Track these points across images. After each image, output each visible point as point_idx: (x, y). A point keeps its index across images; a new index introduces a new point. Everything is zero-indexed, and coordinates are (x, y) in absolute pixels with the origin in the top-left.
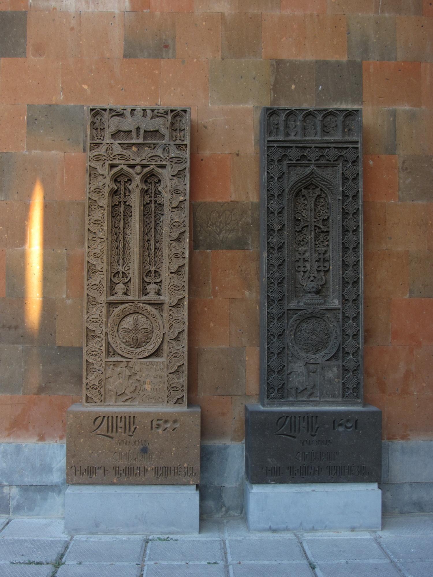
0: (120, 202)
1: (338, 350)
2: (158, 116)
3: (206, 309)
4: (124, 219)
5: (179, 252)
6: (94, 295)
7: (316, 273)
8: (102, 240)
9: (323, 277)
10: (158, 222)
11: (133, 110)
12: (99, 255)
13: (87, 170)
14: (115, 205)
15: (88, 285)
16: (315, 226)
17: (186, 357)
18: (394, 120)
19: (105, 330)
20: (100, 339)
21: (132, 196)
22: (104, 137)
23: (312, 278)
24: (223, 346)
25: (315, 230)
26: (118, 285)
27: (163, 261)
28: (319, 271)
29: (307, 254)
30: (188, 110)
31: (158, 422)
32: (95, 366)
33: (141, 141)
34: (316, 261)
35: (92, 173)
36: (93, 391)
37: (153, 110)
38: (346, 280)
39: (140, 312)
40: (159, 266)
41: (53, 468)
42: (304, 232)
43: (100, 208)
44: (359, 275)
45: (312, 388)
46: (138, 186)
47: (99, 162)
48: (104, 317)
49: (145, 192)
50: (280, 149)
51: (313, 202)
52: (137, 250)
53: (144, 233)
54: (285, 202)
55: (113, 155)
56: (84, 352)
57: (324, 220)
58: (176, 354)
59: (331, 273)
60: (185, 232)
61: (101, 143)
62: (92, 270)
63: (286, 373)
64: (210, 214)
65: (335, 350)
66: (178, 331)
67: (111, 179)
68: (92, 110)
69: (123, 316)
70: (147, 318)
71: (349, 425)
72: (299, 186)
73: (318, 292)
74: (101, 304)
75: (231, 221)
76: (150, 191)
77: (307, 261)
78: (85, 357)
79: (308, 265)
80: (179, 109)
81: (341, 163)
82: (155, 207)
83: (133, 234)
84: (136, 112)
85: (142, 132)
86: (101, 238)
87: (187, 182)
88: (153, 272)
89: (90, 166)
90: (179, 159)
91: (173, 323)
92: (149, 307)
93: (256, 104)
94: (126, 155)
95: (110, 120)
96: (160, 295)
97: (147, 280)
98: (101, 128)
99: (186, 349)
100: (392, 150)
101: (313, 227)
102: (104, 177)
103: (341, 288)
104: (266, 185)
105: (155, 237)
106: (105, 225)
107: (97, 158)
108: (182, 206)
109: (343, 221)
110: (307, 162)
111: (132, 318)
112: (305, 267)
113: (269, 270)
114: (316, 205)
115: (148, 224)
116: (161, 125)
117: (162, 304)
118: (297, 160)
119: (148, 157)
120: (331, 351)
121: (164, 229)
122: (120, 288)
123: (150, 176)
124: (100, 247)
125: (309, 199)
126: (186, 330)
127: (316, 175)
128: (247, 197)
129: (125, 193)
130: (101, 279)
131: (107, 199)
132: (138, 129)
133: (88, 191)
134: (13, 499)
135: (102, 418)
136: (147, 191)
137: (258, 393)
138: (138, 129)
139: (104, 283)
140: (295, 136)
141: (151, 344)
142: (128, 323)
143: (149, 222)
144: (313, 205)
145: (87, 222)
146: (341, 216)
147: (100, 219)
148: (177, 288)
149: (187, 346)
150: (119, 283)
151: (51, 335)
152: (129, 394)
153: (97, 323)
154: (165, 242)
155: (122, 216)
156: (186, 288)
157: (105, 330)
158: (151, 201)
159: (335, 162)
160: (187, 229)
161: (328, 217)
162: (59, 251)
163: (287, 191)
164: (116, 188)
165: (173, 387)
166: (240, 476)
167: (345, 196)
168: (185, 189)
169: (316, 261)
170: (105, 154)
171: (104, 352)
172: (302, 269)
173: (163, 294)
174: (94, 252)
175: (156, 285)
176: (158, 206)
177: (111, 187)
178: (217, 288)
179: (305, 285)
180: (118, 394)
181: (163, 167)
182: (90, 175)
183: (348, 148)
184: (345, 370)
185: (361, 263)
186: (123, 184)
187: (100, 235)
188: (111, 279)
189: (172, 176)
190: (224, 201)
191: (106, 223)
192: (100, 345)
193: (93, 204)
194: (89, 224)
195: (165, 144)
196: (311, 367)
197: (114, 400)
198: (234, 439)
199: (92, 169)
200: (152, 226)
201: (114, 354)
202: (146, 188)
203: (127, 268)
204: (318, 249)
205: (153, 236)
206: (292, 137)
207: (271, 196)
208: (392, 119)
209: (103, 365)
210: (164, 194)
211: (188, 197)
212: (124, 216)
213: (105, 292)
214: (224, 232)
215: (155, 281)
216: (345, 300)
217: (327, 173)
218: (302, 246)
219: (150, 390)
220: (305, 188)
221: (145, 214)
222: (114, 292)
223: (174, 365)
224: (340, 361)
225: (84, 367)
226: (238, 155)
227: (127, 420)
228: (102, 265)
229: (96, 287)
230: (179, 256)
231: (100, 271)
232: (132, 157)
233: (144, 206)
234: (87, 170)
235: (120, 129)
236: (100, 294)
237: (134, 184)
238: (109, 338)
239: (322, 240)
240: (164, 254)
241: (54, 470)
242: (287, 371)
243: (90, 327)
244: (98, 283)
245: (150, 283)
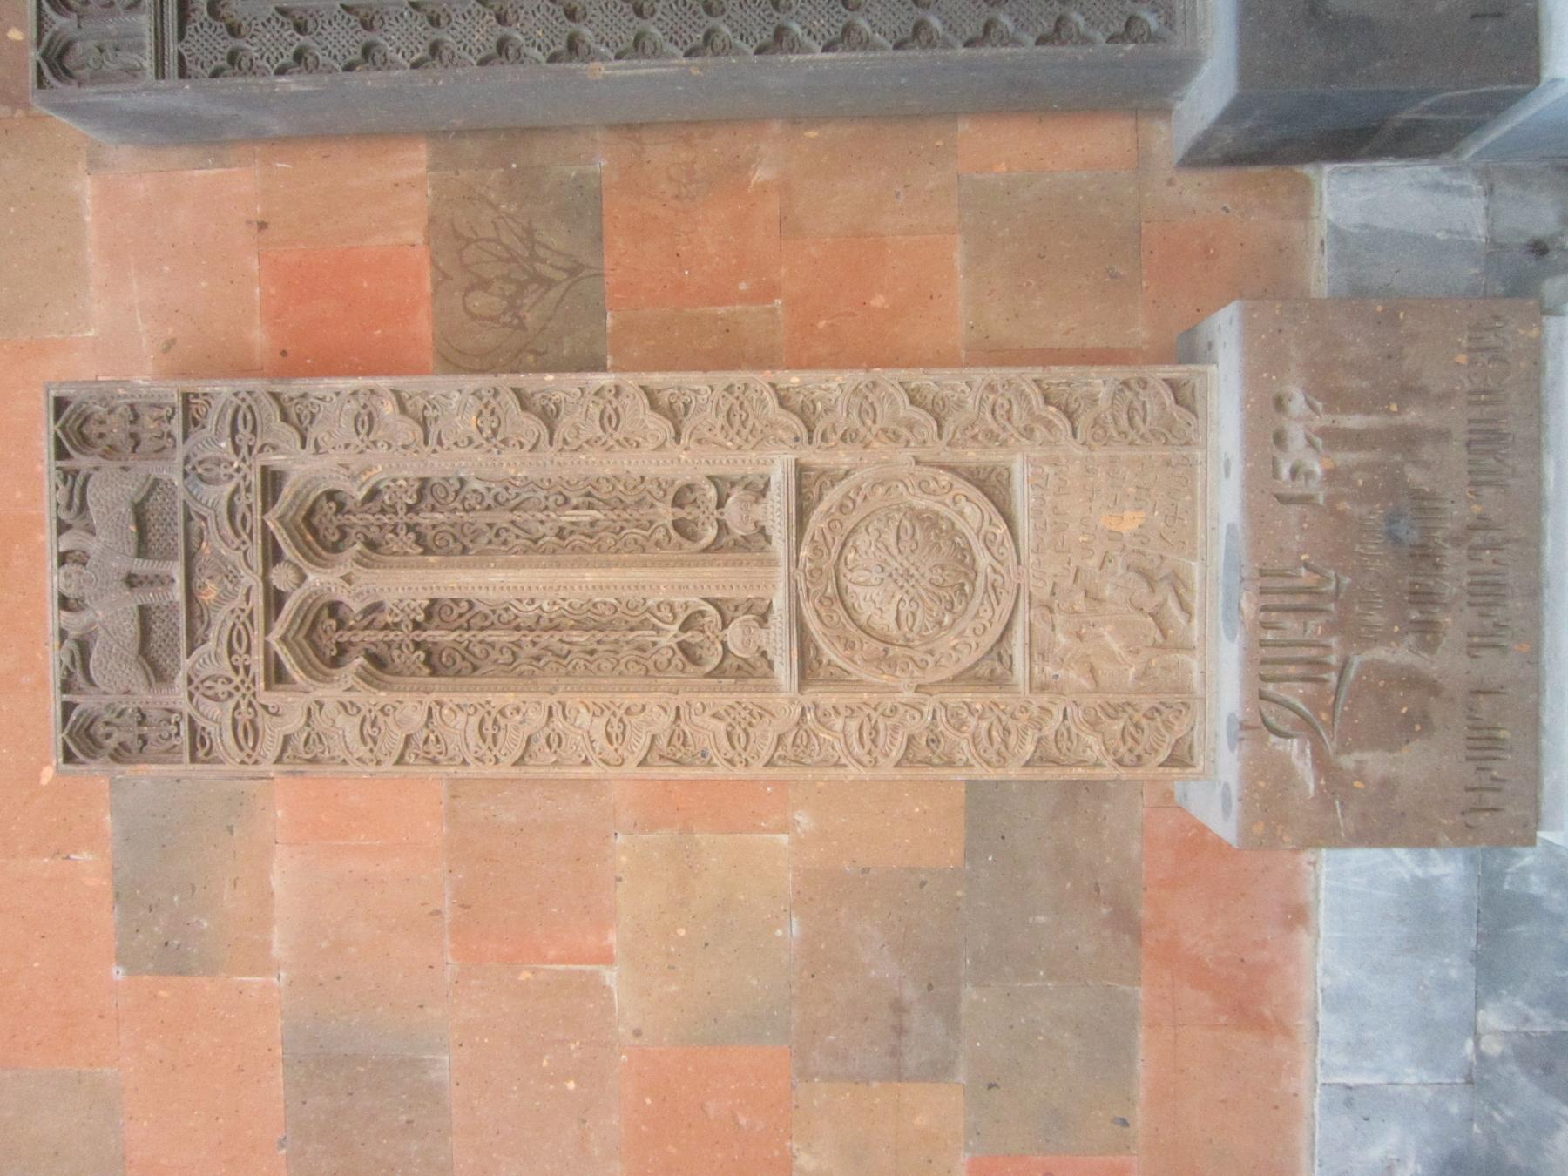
0: (417, 645)
2: (83, 507)
3: (822, 324)
4: (482, 629)
5: (595, 411)
6: (772, 738)
8: (557, 710)
10: (489, 500)
11: (64, 603)
12: (615, 721)
13: (293, 773)
14: (427, 662)
15: (730, 761)
17: (1012, 372)
19: (908, 695)
20: (941, 714)
21: (389, 600)
22: (171, 711)
24: (959, 259)
26: (730, 647)
27: (636, 474)
30: (53, 393)
31: (1285, 472)
32: (1050, 728)
33: (177, 571)
35: (303, 753)
36: (1147, 738)
37: (63, 527)
39: (834, 556)
40: (653, 488)
41: (1414, 877)
43: (436, 720)
46: (347, 579)
47: (260, 725)
48: (853, 700)
52: (590, 576)
55: (231, 674)
56: (994, 774)
58: (998, 412)
60: (517, 392)
61: (192, 721)
62: (675, 748)
64: (473, 317)
66: (906, 410)
67: (326, 679)
68: (69, 757)
69: (851, 628)
70: (854, 531)
74: (803, 713)
75: (498, 241)
76: (374, 533)
78: (1014, 772)
80: (53, 427)
82: (433, 509)
83: (534, 593)
84: (69, 593)
85: (142, 567)
86: (550, 714)
87: (324, 386)
88: (680, 513)
89: (278, 761)
90: (240, 421)
91: (875, 428)
92: (816, 522)
93: (82, 166)
94: (230, 624)
95: (103, 688)
96: (767, 484)
97: (711, 533)
98: (140, 724)
99: (980, 376)
102: (315, 709)
105: (546, 508)
106: (497, 700)
107: (246, 733)
108: (422, 402)
111: (858, 589)
113: (657, 53)
115: (497, 535)
116: (111, 492)
117: (801, 470)
119: (237, 542)
121: (512, 472)
123: (315, 532)
124: (584, 718)
126: (902, 374)
128: (412, 185)
129: (386, 627)
130: (708, 711)
131: (400, 696)
132: (131, 581)
133: (372, 768)
134: (1527, 1020)
135: (1264, 705)
136: (372, 545)
137: (1131, 122)
138: (131, 581)
139: (725, 700)
141: (961, 514)
142: (874, 601)
143: (491, 534)
145: (489, 770)
147: (474, 721)
148: (735, 416)
149: (966, 371)
150: (724, 644)
151: (923, 884)
152: (1158, 598)
153: (881, 727)
154: (555, 465)
155: (467, 635)
156: (736, 377)
157: (908, 695)
158: (410, 528)
160: (505, 380)
162: (624, 859)
164: (361, 660)
165: (1130, 419)
166: (1445, 178)
168: (354, 393)
170: (231, 704)
171: (996, 697)
173: (762, 469)
174: (601, 741)
175: (730, 500)
176: (429, 500)
177: (351, 680)
178: (743, 286)
180: (1160, 640)
181: (272, 481)
182: (313, 761)
186: (345, 637)
187: (538, 718)
188: (709, 675)
189: (303, 446)
190: (428, 272)
191: (489, 696)
192: (965, 714)
194: (497, 761)
195: (186, 475)
197: (1181, 657)
198: (1303, 212)
199: (290, 752)
200: (502, 518)
201: (1000, 659)
202: (358, 547)
203: (665, 613)
205: (540, 516)
209: (1044, 699)
210: (378, 474)
211: (383, 383)
212: (469, 629)
213: (759, 698)
214: (538, 265)
215: (713, 504)
219: (1142, 514)
221: (458, 545)
222: (761, 664)
223: (1040, 419)
225: (1052, 773)
226: (262, 226)
227: (1275, 600)
228: (653, 711)
229: (738, 730)
230: (609, 410)
231: (678, 716)
232: (239, 602)
233: (427, 551)
234: (293, 773)
235: (135, 648)
236: (767, 718)
237: (341, 594)
238: (938, 677)
240: (608, 471)
241: (1419, 872)
243: (896, 753)
244: (722, 726)
245: (722, 527)
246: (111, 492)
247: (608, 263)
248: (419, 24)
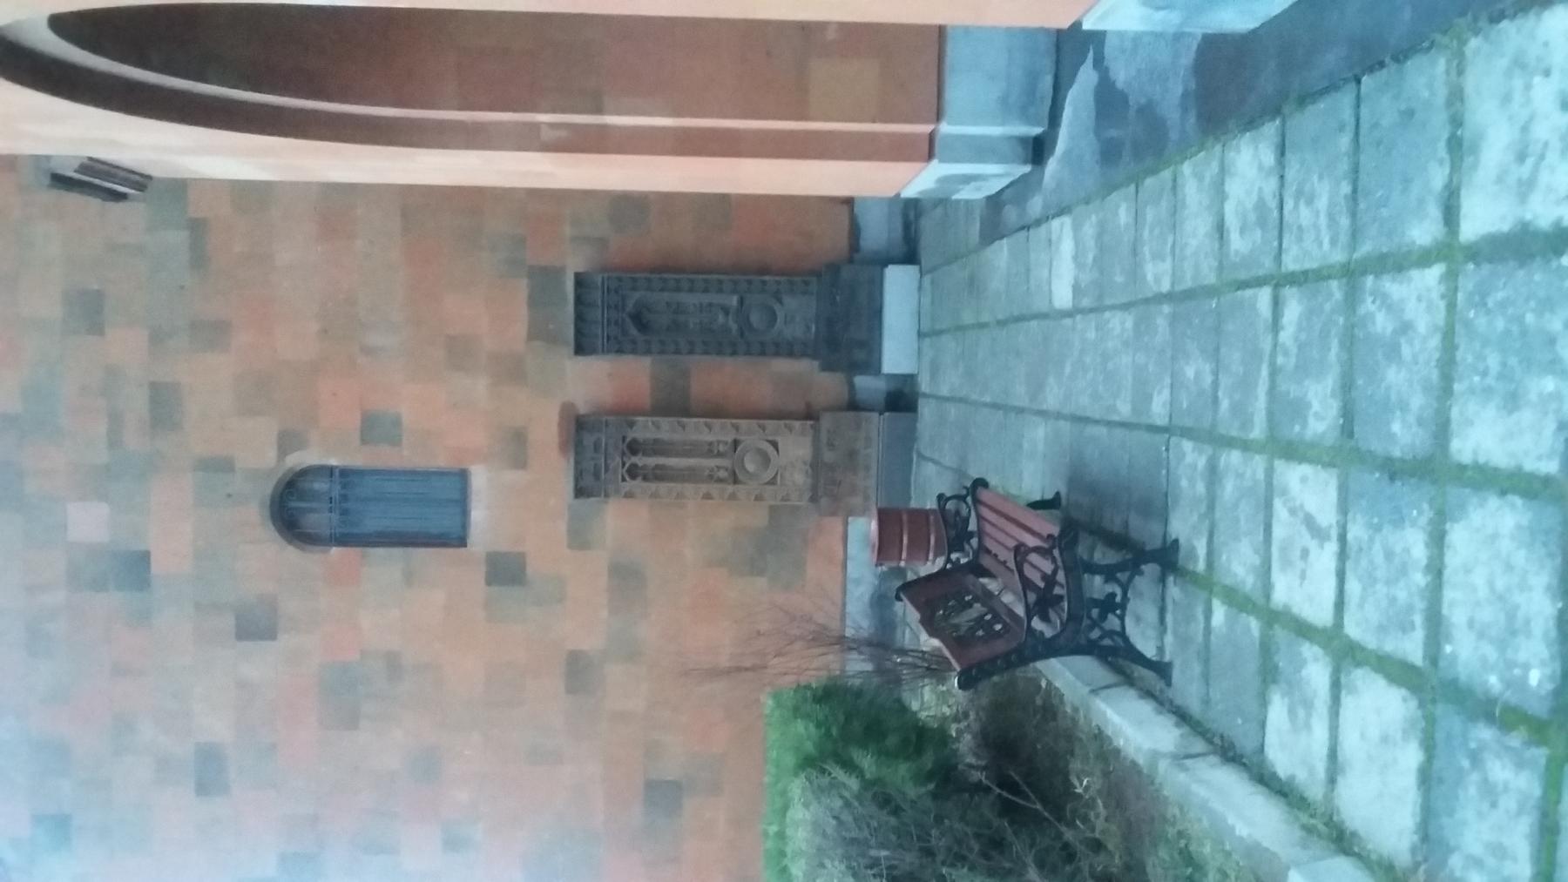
35: (629, 495)
49: (645, 454)
53: (678, 455)
122: (722, 474)
130: (714, 489)
142: (750, 467)
193: (654, 495)
216: (734, 292)
228: (704, 488)
246: (589, 440)
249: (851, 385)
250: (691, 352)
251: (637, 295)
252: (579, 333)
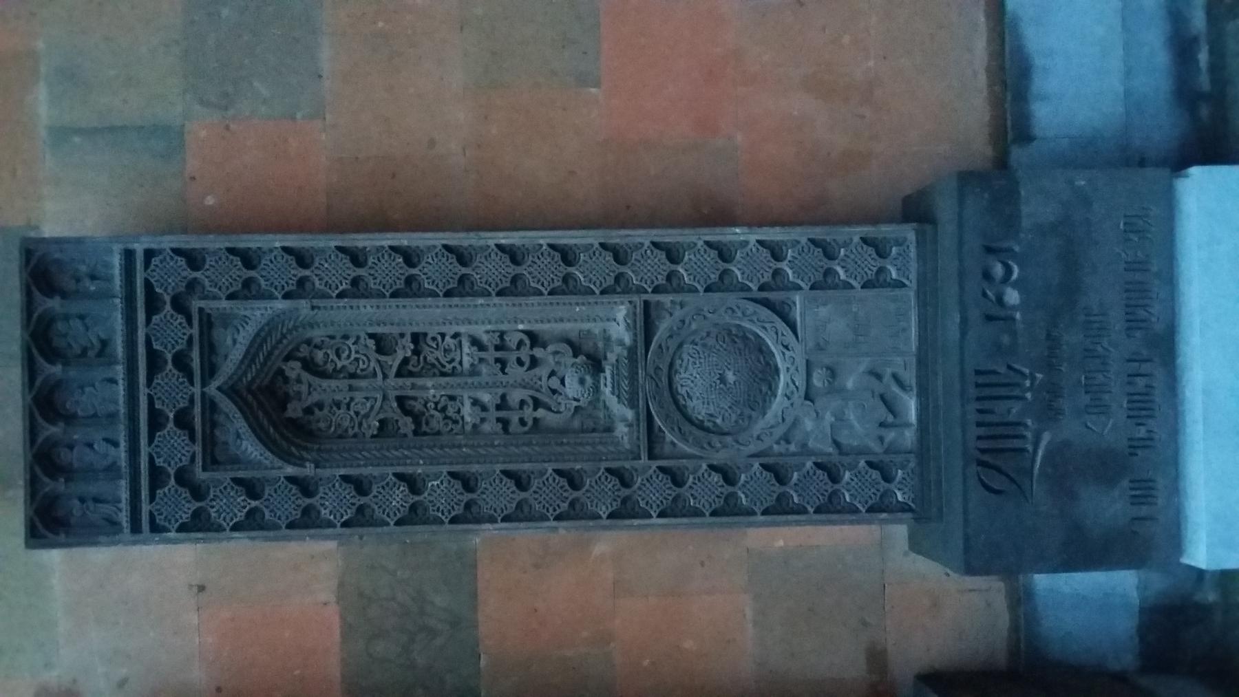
1: (766, 303)
7: (537, 371)
9: (551, 348)
16: (399, 374)
18: (79, 131)
23: (554, 382)
25: (411, 374)
28: (534, 362)
29: (486, 397)
34: (503, 370)
38: (557, 284)
42: (418, 406)
44: (541, 246)
45: (879, 377)
50: (159, 492)
51: (325, 383)
54: (326, 473)
57: (380, 350)
59: (536, 327)
63: (836, 458)
65: (765, 313)
71: (998, 270)
72: (275, 428)
73: (595, 364)
75: (393, 599)
77: (503, 397)
79: (516, 396)
81: (196, 304)
100: (169, 138)
101: (400, 381)
103: (579, 299)
104: (271, 534)
109: (381, 295)
110: (197, 410)
112: (522, 403)
114: (335, 374)
118: (192, 438)
120: (767, 325)
125: (316, 397)
127: (240, 379)
140: (116, 444)
144: (333, 383)
146: (362, 302)
159: (196, 322)
161: (371, 336)
163: (290, 470)
167: (300, 289)
169: (503, 370)
172: (528, 412)
179: (575, 404)
183: (148, 285)
184: (824, 283)
185: (505, 238)
196: (817, 382)
204: (466, 365)
206: (122, 454)
207: (307, 521)
208: (77, 139)
216: (618, 287)
217: (234, 348)
218: (459, 411)
220: (284, 409)
224: (797, 298)
226: (202, 588)
239: (439, 354)
242: (830, 454)
247: (481, 618)
248: (348, 491)
249: (1021, 600)
250: (469, 516)
251: (257, 313)
252: (45, 462)
